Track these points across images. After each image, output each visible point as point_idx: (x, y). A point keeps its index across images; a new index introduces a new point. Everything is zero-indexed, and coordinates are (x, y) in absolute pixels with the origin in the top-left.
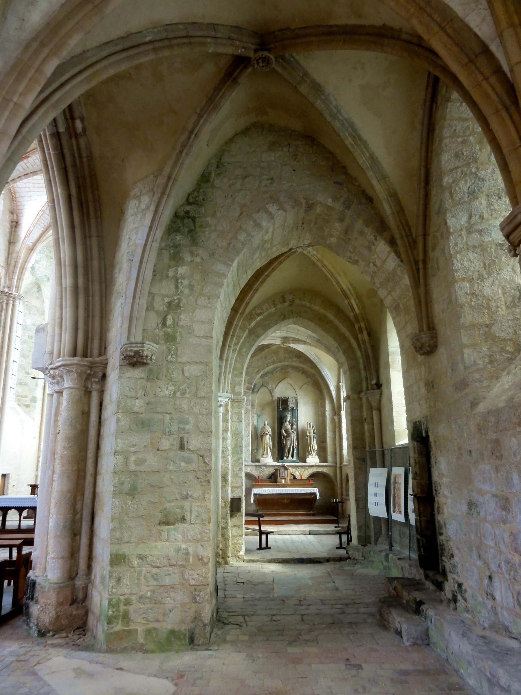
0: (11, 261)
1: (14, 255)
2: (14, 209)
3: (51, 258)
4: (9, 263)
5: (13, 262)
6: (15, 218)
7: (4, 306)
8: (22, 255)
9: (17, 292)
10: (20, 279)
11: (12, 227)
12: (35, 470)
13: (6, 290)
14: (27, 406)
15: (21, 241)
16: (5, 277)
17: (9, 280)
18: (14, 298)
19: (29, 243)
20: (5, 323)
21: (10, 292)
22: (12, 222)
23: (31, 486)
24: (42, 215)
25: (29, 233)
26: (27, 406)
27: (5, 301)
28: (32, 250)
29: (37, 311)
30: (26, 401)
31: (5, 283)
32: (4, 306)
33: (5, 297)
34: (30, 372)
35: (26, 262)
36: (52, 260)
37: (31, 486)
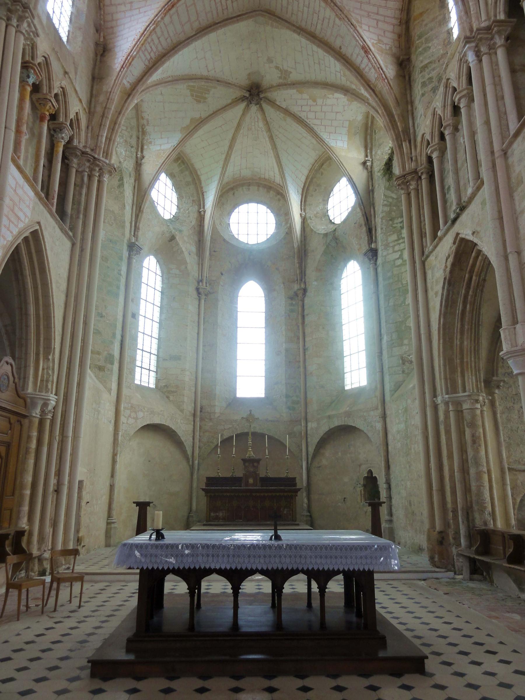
0: (95, 107)
1: (102, 98)
2: (100, 25)
3: (132, 147)
4: (92, 110)
5: (99, 109)
6: (102, 40)
7: (86, 179)
8: (116, 97)
9: (106, 158)
10: (110, 140)
11: (96, 55)
12: (110, 475)
13: (88, 150)
14: (101, 369)
15: (115, 74)
16: (87, 133)
17: (92, 137)
18: (100, 169)
19: (127, 82)
20: (86, 209)
21: (96, 156)
22: (97, 44)
23: (138, 504)
24: (154, 29)
25: (130, 60)
26: (101, 369)
27: (87, 170)
28: (129, 95)
29: (115, 220)
30: (99, 360)
31: (86, 142)
32: (86, 179)
33: (88, 164)
34: (104, 314)
35: (119, 114)
36: (132, 150)
37: (138, 504)
